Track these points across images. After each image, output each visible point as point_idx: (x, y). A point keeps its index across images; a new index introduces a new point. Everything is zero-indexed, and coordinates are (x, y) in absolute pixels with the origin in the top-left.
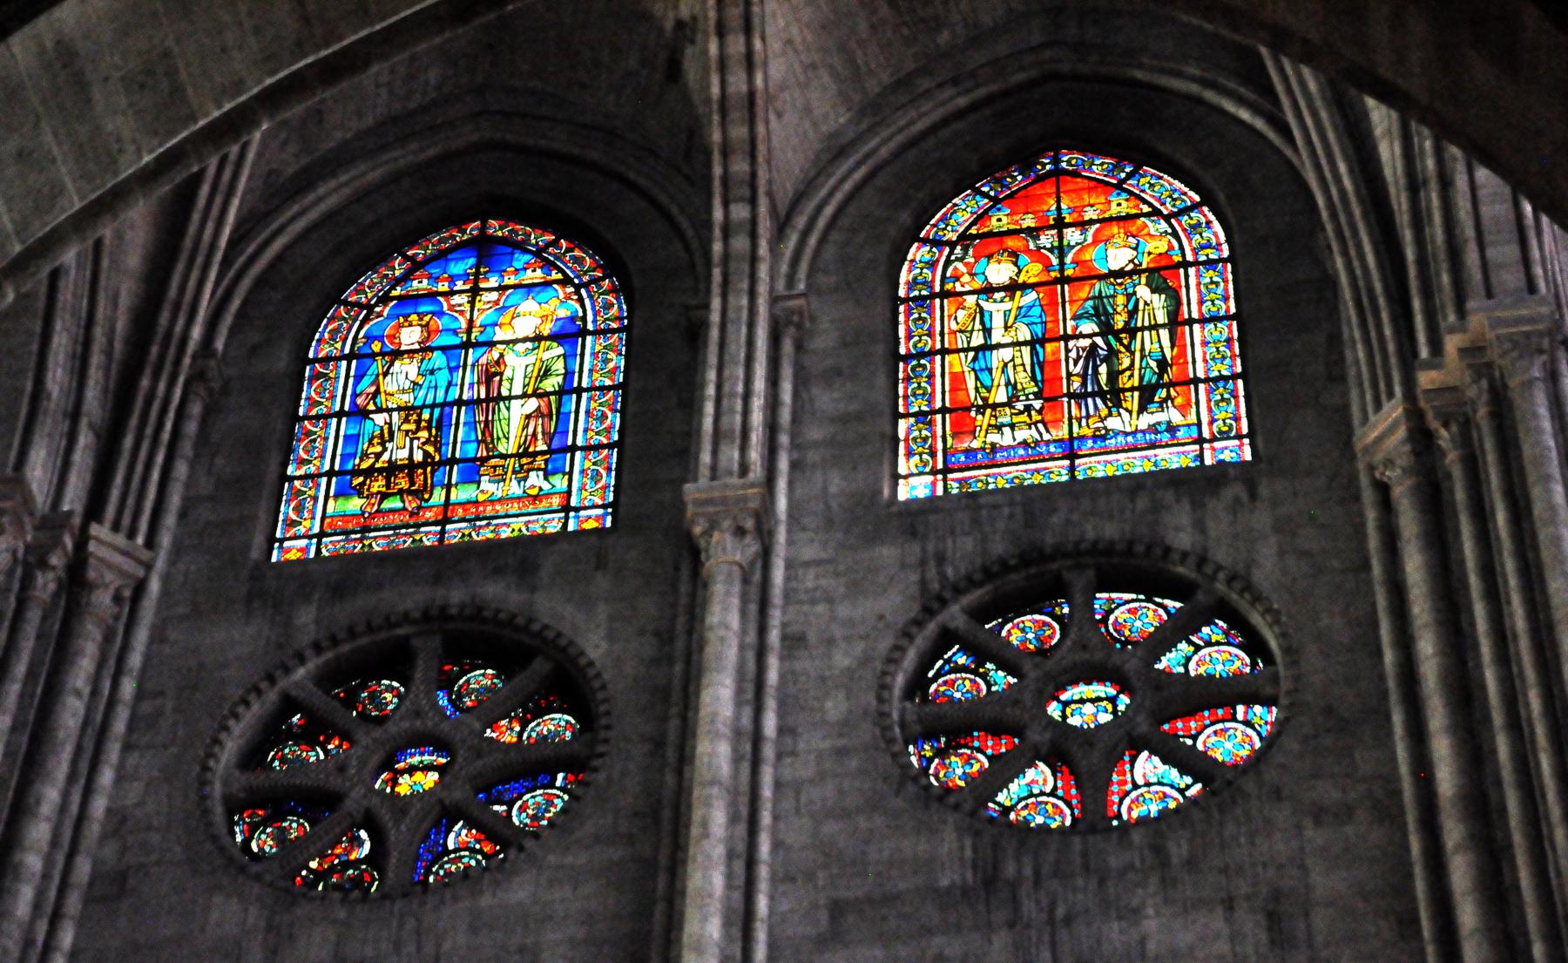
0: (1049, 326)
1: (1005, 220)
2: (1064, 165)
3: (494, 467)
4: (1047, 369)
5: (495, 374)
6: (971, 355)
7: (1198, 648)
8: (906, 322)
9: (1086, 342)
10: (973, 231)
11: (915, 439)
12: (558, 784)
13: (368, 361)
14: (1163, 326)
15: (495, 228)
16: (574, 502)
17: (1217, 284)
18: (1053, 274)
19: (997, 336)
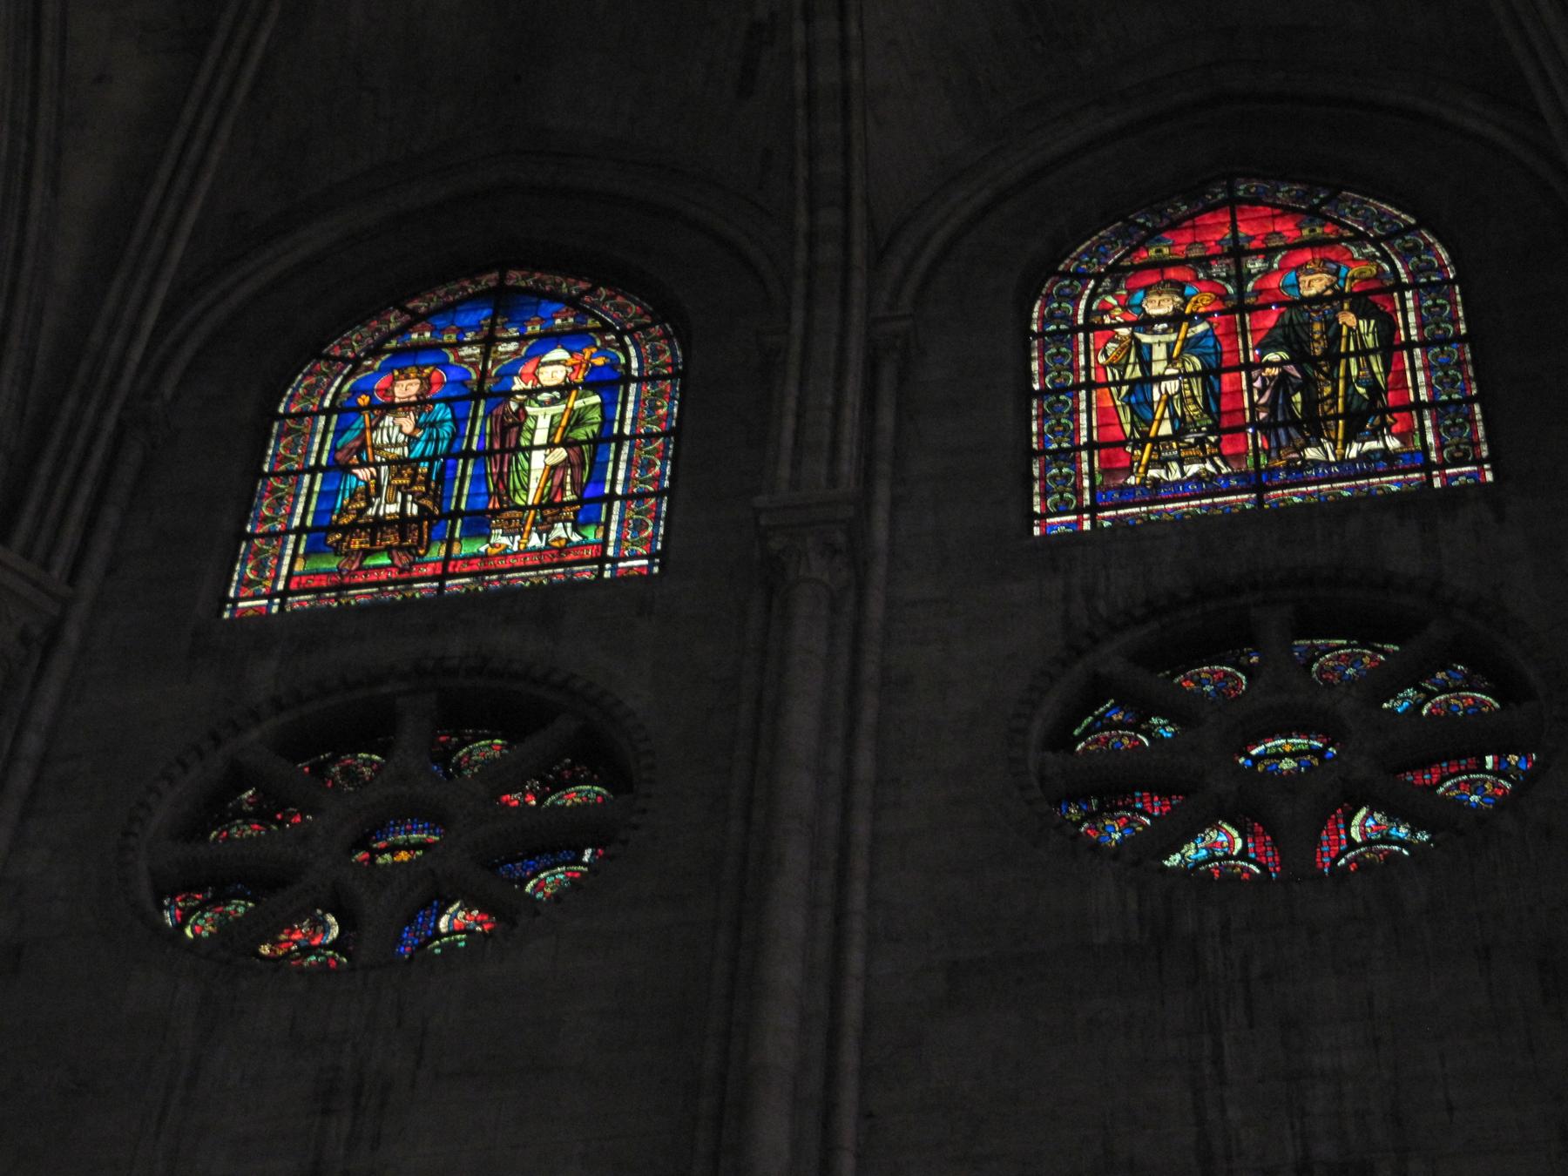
0: (1225, 356)
1: (1166, 251)
2: (1241, 193)
3: (510, 520)
4: (1224, 400)
5: (513, 425)
6: (1125, 389)
7: (1430, 695)
8: (1041, 357)
9: (1275, 371)
10: (1126, 263)
11: (1053, 478)
12: (586, 859)
13: (351, 416)
14: (1374, 351)
15: (515, 278)
16: (610, 552)
17: (1443, 307)
18: (1230, 304)
19: (1157, 369)
